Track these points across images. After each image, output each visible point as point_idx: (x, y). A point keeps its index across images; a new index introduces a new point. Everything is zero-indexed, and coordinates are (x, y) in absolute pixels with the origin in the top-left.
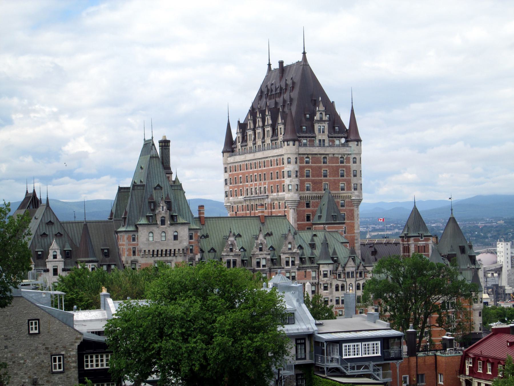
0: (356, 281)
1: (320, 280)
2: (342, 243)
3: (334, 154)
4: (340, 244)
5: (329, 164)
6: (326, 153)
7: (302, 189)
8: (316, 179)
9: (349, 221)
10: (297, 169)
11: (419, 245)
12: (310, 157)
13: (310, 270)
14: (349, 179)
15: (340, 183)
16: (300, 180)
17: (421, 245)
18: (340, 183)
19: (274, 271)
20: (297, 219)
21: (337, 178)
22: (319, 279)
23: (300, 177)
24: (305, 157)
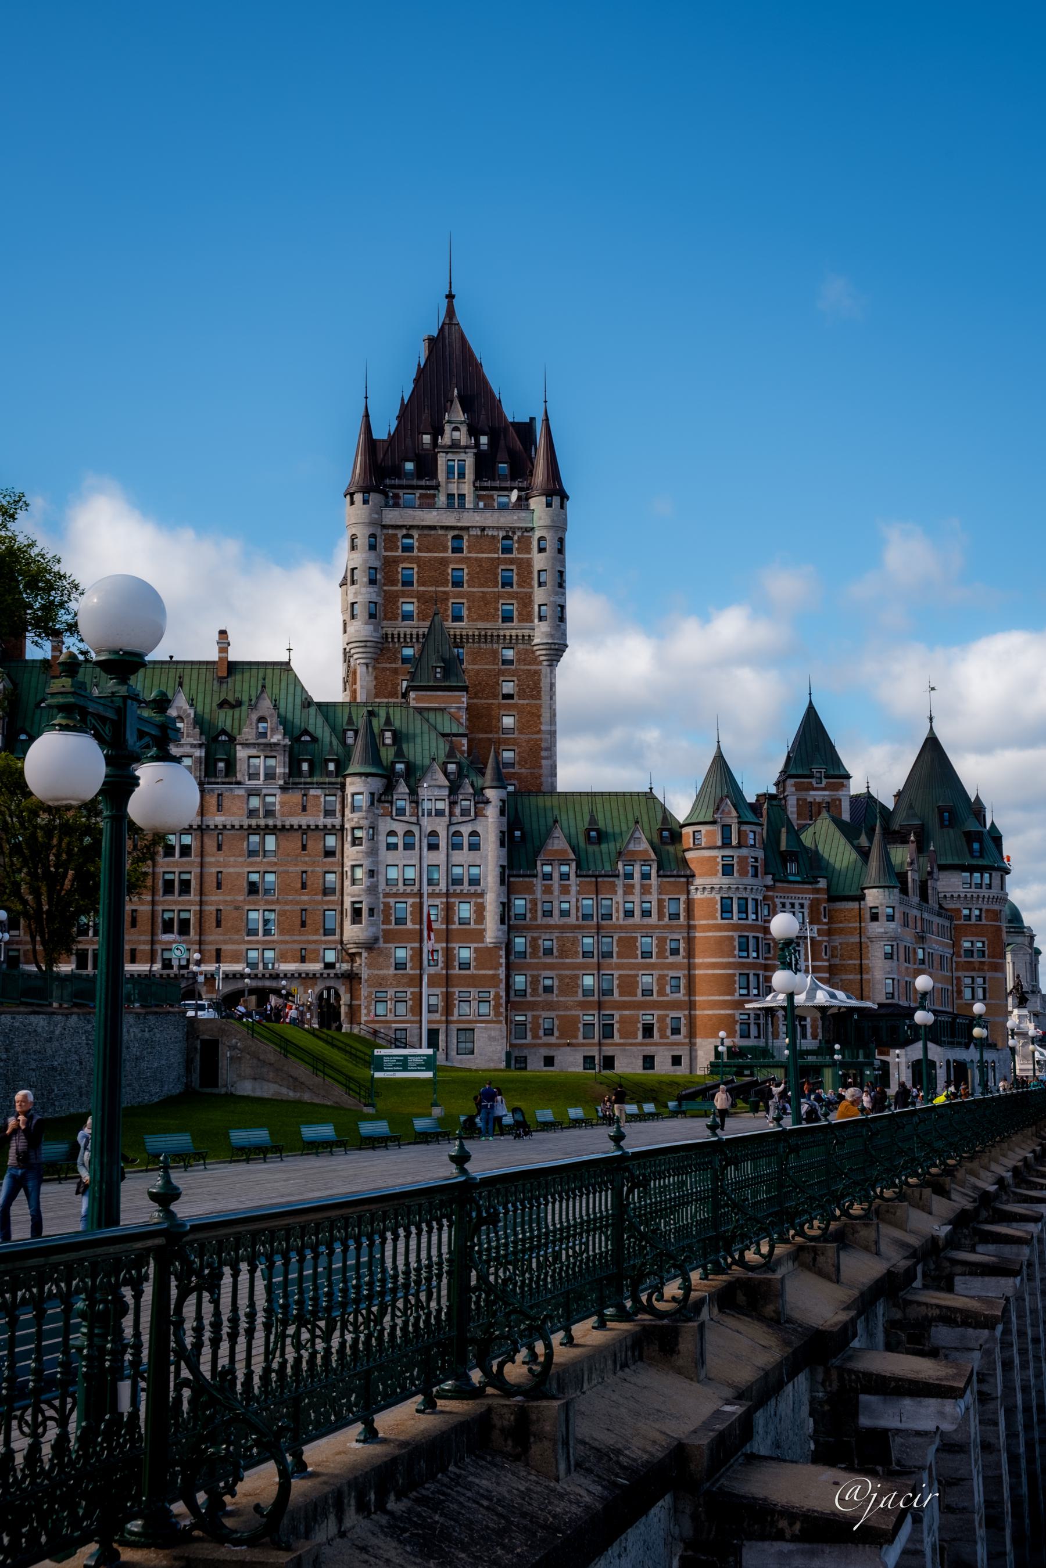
0: (451, 824)
1: (346, 819)
2: (444, 735)
3: (483, 529)
4: (433, 735)
5: (469, 552)
6: (459, 524)
7: (390, 615)
8: (430, 592)
9: (526, 701)
10: (377, 564)
11: (810, 799)
12: (415, 534)
13: (319, 792)
14: (526, 593)
15: (501, 601)
16: (385, 591)
17: (818, 800)
18: (501, 601)
19: (212, 790)
20: (374, 691)
21: (490, 590)
22: (343, 815)
23: (385, 585)
24: (400, 536)
